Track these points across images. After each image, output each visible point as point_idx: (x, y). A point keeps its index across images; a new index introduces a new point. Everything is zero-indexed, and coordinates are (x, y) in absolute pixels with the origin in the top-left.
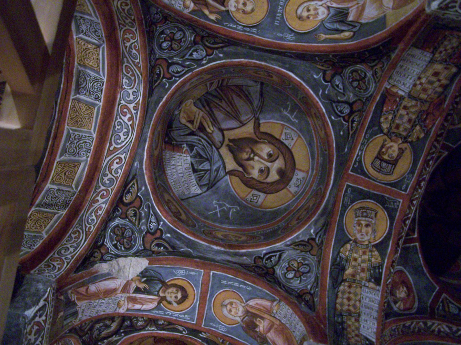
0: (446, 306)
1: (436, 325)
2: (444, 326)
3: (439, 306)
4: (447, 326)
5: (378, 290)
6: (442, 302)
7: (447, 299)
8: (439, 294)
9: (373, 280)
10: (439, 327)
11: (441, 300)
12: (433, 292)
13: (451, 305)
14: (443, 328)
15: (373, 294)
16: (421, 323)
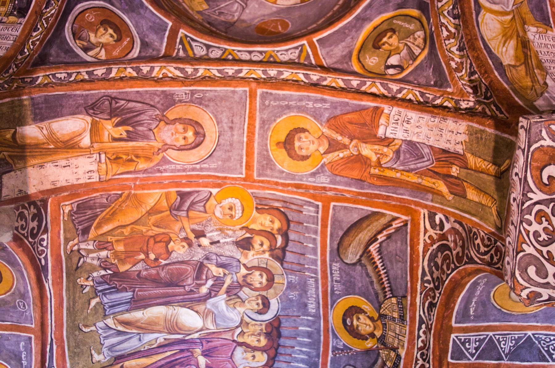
0: (187, 47)
1: (157, 69)
2: (172, 69)
3: (179, 50)
4: (175, 68)
5: (21, 24)
6: (181, 42)
7: (186, 36)
8: (174, 33)
9: (15, 13)
10: (164, 71)
11: (178, 40)
12: (165, 30)
13: (194, 44)
14: (171, 72)
15: (10, 29)
16: (129, 70)
